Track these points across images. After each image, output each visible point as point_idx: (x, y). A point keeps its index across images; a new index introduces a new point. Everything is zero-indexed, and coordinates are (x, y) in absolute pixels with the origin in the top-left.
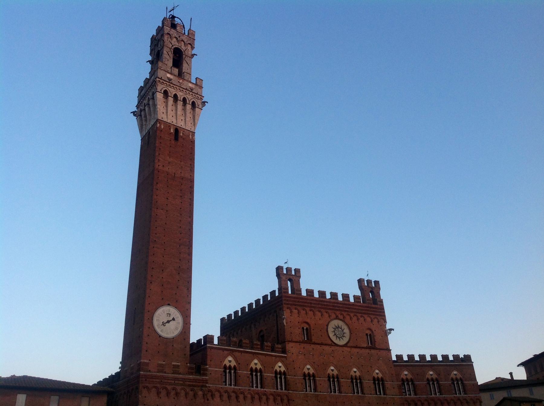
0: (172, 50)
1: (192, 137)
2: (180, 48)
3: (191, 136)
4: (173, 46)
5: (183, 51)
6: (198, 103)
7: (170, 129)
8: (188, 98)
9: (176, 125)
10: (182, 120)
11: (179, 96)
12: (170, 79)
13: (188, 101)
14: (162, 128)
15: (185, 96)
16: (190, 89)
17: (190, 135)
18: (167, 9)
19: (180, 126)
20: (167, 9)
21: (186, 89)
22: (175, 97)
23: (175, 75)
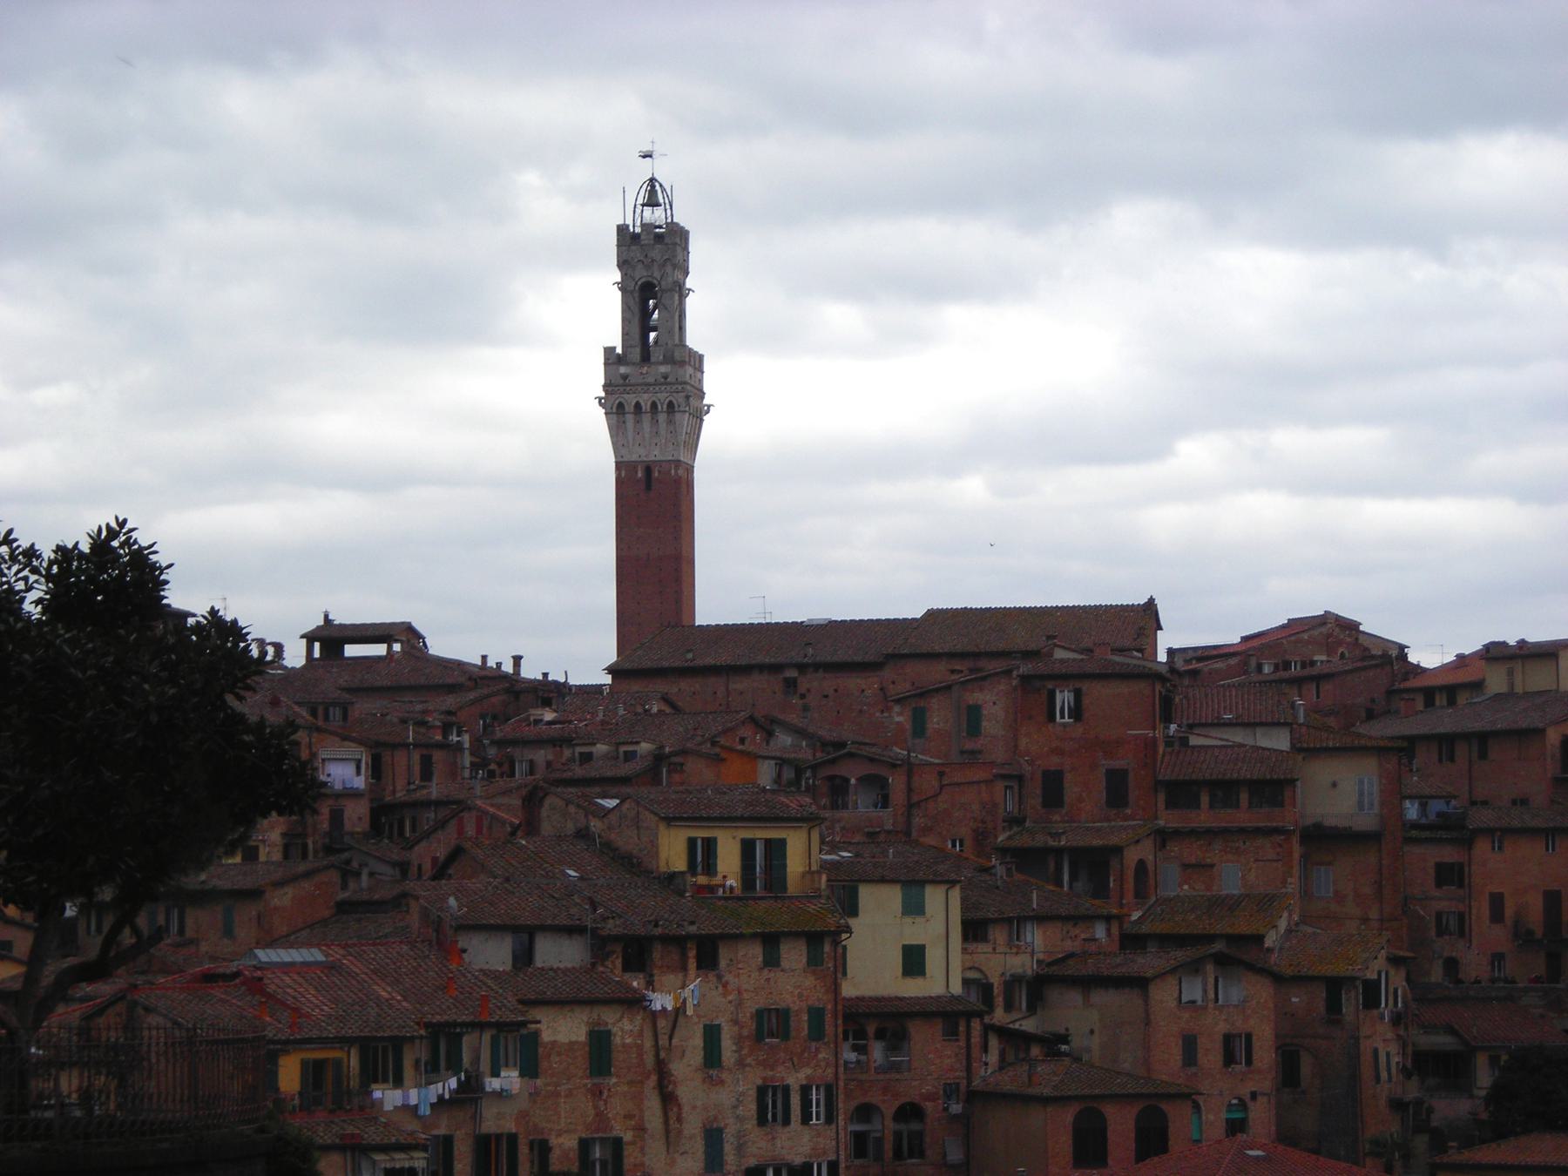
0: (636, 295)
1: (676, 471)
2: (650, 279)
3: (673, 471)
4: (636, 283)
5: (655, 282)
6: (680, 400)
7: (636, 472)
8: (659, 400)
9: (645, 459)
10: (656, 444)
11: (643, 404)
12: (625, 377)
13: (660, 407)
14: (623, 475)
15: (654, 399)
16: (663, 377)
17: (670, 470)
18: (624, 192)
19: (654, 458)
20: (624, 192)
21: (656, 384)
22: (638, 406)
23: (634, 364)
